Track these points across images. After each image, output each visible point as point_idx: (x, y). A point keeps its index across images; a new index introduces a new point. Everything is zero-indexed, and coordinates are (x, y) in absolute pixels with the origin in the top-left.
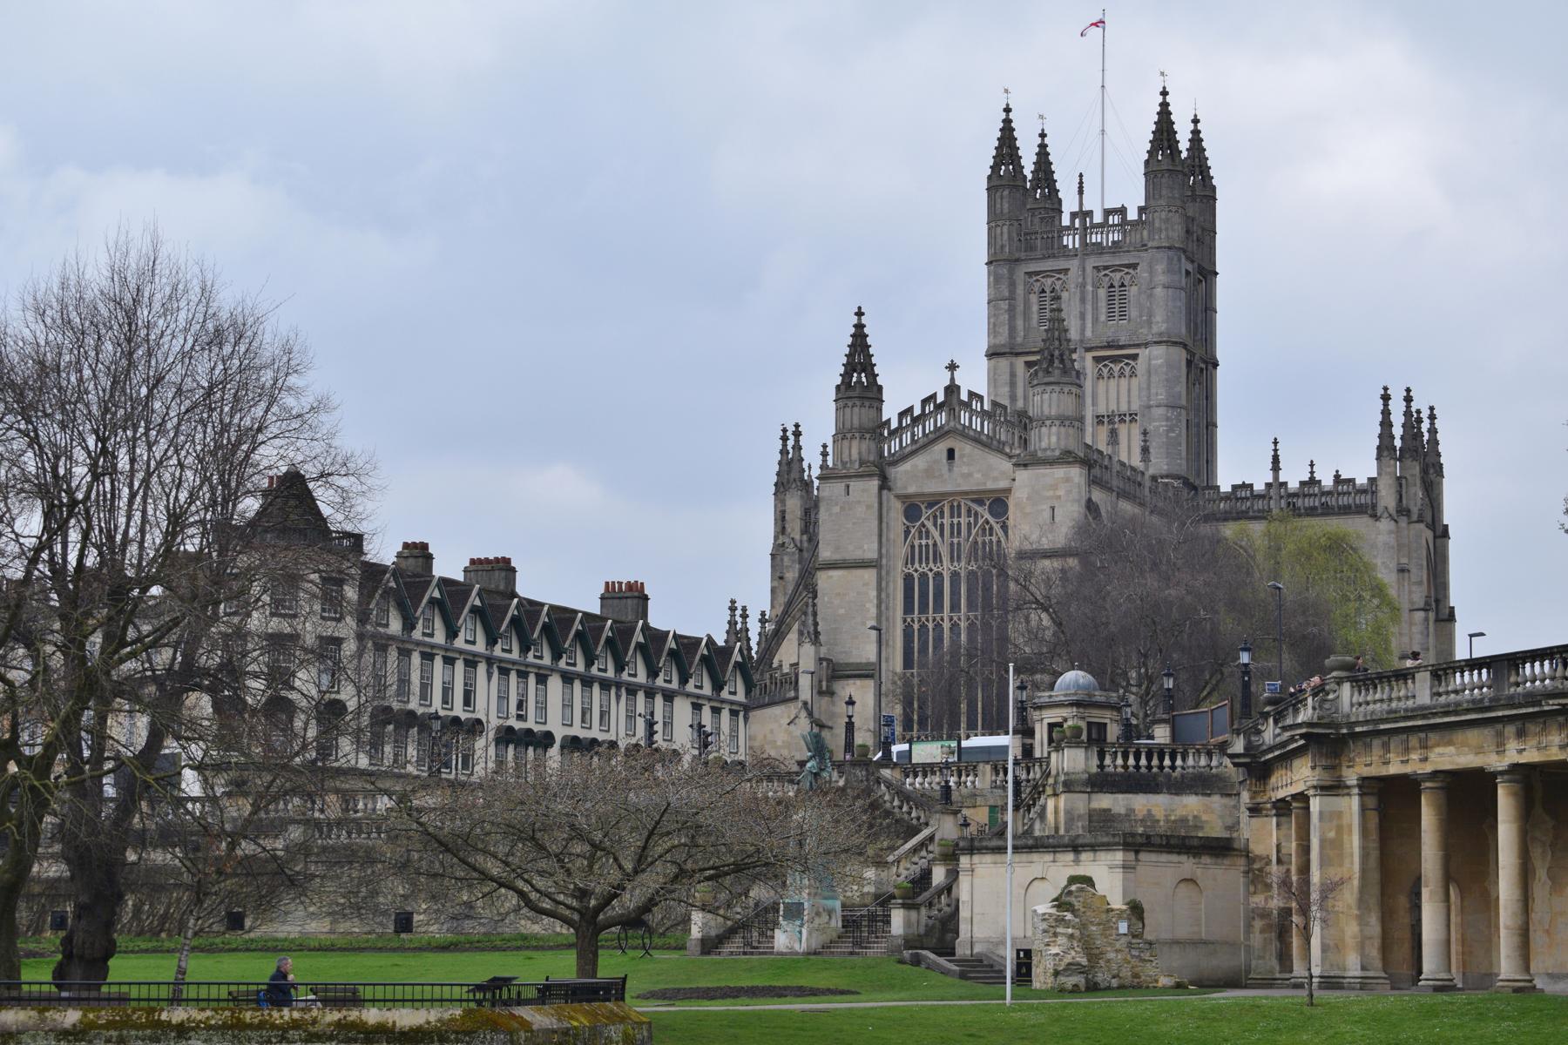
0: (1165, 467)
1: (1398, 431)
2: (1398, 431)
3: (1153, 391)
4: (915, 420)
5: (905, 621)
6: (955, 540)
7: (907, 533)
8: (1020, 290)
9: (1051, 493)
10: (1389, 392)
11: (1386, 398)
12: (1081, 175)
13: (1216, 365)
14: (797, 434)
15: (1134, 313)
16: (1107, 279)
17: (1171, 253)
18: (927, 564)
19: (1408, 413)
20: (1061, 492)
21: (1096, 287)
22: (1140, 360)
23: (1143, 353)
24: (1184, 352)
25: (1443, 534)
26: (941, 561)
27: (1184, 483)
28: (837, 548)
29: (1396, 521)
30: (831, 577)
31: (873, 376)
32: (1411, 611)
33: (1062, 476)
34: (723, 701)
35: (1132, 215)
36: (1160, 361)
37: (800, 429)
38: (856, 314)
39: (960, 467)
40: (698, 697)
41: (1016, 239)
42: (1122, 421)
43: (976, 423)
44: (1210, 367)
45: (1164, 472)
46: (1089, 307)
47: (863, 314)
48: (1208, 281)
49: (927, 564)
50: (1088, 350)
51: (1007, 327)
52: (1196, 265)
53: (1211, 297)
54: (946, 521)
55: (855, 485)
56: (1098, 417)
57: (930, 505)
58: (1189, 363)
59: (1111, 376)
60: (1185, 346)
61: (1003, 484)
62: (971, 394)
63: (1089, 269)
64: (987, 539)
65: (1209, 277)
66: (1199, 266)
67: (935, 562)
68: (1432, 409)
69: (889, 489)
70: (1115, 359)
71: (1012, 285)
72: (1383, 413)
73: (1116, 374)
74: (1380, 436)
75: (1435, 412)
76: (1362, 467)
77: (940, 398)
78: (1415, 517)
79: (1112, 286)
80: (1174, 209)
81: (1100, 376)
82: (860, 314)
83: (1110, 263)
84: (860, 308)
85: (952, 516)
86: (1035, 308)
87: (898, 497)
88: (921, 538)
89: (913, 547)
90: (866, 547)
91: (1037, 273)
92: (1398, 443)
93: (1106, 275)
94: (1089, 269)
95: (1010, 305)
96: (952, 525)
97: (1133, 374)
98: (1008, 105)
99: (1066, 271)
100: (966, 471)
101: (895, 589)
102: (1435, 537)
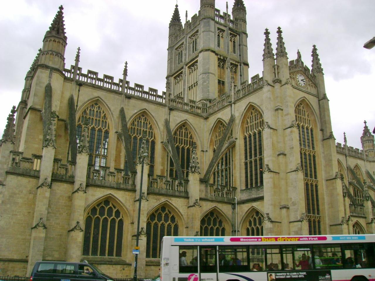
0: (202, 97)
1: (274, 46)
2: (274, 46)
10: (268, 31)
11: (267, 33)
12: (187, 11)
19: (280, 38)
24: (213, 54)
29: (274, 87)
46: (187, 51)
50: (186, 65)
58: (222, 61)
60: (213, 52)
70: (193, 65)
80: (207, 6)
92: (275, 52)
94: (188, 39)
95: (171, 61)
99: (183, 43)
102: (319, 101)
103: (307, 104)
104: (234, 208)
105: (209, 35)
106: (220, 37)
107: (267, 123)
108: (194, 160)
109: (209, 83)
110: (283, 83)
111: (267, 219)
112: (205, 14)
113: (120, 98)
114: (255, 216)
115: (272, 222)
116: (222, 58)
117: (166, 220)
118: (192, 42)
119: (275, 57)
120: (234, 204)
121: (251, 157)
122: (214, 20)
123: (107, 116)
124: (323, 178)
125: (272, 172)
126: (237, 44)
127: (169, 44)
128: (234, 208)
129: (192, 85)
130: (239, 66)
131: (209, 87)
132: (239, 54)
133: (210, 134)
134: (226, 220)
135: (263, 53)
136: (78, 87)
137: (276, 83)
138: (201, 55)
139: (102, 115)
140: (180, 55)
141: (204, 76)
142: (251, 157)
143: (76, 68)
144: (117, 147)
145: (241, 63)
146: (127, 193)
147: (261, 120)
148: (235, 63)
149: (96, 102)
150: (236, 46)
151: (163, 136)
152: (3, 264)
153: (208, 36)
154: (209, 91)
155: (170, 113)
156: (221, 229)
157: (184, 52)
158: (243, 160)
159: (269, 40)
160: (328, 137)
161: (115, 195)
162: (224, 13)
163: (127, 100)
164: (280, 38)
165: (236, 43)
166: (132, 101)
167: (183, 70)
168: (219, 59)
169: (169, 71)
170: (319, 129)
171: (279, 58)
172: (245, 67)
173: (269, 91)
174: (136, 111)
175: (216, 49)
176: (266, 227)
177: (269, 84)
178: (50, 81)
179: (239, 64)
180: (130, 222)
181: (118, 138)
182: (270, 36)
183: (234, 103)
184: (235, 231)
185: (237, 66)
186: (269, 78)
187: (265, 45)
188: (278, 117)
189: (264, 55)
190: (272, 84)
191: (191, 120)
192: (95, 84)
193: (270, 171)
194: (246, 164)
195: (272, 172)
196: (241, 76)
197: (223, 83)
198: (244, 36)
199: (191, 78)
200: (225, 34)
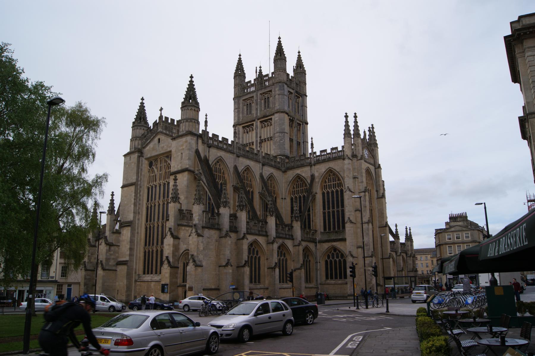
1: (352, 128)
2: (352, 128)
3: (276, 128)
8: (241, 105)
11: (346, 117)
13: (307, 124)
15: (271, 105)
16: (264, 97)
17: (280, 84)
19: (356, 122)
21: (261, 100)
22: (273, 119)
23: (273, 117)
24: (286, 116)
27: (286, 157)
29: (352, 160)
32: (359, 193)
33: (185, 140)
35: (270, 76)
36: (277, 119)
38: (141, 99)
39: (161, 145)
41: (240, 90)
42: (268, 140)
44: (304, 124)
45: (279, 154)
46: (259, 106)
47: (144, 99)
48: (303, 98)
50: (258, 119)
51: (237, 117)
52: (295, 91)
53: (304, 103)
58: (291, 121)
59: (265, 126)
60: (287, 113)
63: (259, 94)
65: (303, 96)
66: (296, 91)
68: (372, 125)
69: (143, 157)
70: (266, 121)
71: (239, 104)
72: (345, 122)
73: (266, 126)
74: (345, 130)
75: (373, 126)
76: (339, 142)
78: (359, 158)
79: (265, 99)
80: (281, 70)
81: (262, 127)
82: (143, 99)
84: (143, 97)
86: (245, 110)
87: (145, 159)
91: (245, 99)
92: (352, 132)
93: (264, 96)
94: (259, 94)
95: (238, 110)
97: (271, 125)
99: (253, 96)
100: (162, 146)
101: (143, 193)
102: (375, 169)
103: (369, 171)
104: (316, 246)
105: (284, 98)
106: (290, 99)
107: (348, 187)
108: (296, 212)
109: (284, 141)
110: (359, 158)
111: (349, 255)
112: (280, 78)
113: (233, 157)
114: (333, 252)
115: (353, 257)
116: (291, 118)
117: (281, 256)
118: (264, 99)
119: (352, 136)
120: (316, 243)
121: (329, 208)
122: (286, 84)
123: (225, 172)
124: (378, 226)
125: (353, 223)
126: (300, 105)
127: (235, 94)
128: (316, 246)
129: (266, 139)
130: (302, 125)
131: (285, 145)
132: (301, 114)
133: (289, 185)
134: (312, 254)
135: (343, 132)
136: (208, 148)
137: (354, 157)
138: (276, 115)
139: (222, 171)
140: (249, 106)
141: (280, 135)
142: (329, 208)
143: (205, 132)
144: (233, 198)
145: (303, 122)
146: (263, 238)
147: (339, 182)
148: (299, 122)
149: (220, 160)
150: (299, 107)
151: (259, 187)
152: (208, 292)
153: (283, 100)
154: (285, 148)
155: (262, 168)
156: (308, 260)
157: (253, 105)
158: (322, 210)
159: (348, 122)
160: (381, 196)
161: (258, 239)
162: (291, 76)
163: (237, 159)
164: (356, 122)
165: (299, 104)
166: (241, 159)
167: (254, 123)
168: (290, 119)
169: (237, 119)
170: (375, 190)
171: (356, 139)
172: (306, 125)
173: (349, 164)
174: (243, 168)
175: (288, 112)
176: (349, 261)
177: (349, 158)
178: (197, 146)
179: (302, 123)
180: (265, 259)
181: (234, 191)
182: (349, 119)
183: (314, 165)
184: (317, 262)
185: (300, 125)
186: (348, 153)
187: (345, 126)
188: (356, 184)
189: (344, 134)
190: (351, 158)
191: (277, 174)
192: (222, 147)
193: (351, 222)
194: (324, 213)
195: (353, 223)
196: (303, 133)
197: (292, 139)
198: (305, 97)
199: (264, 132)
200: (293, 96)
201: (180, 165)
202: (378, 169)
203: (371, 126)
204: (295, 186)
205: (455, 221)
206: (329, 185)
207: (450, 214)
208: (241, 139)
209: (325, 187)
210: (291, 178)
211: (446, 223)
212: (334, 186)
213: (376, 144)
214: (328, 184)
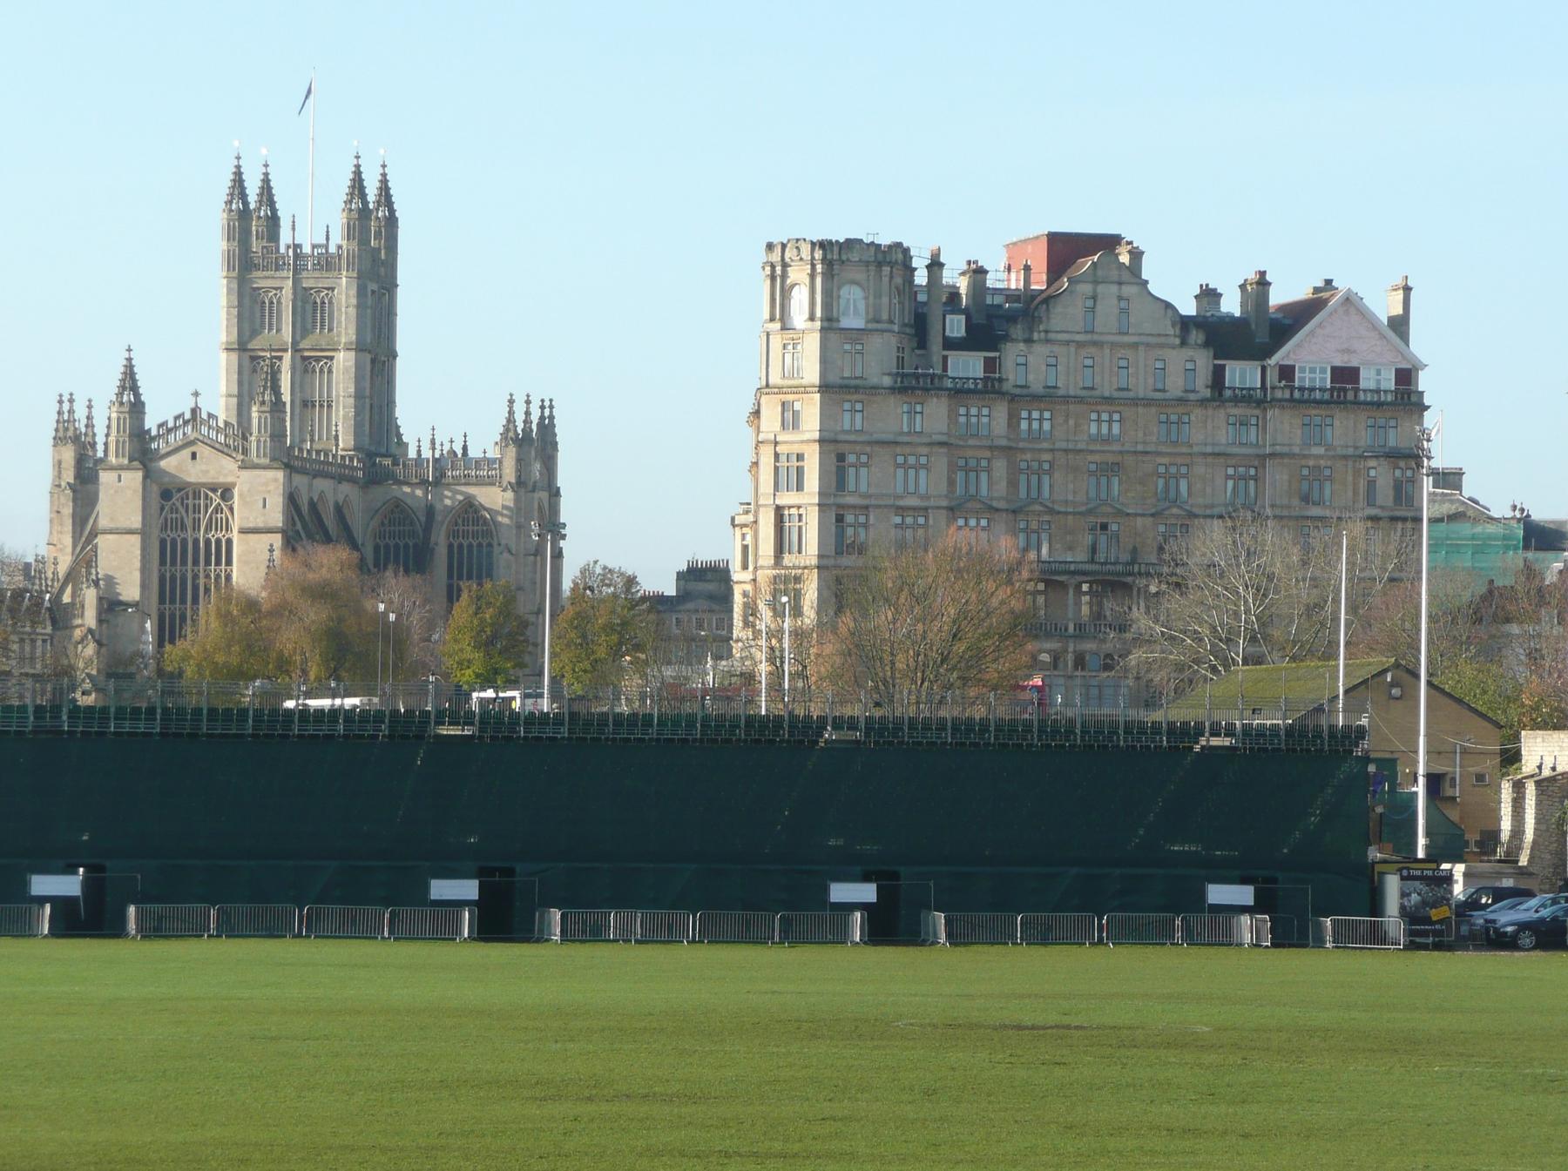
1: (520, 426)
4: (169, 431)
5: (160, 570)
6: (197, 516)
7: (162, 509)
9: (264, 488)
11: (511, 402)
13: (395, 356)
14: (71, 401)
18: (176, 531)
20: (271, 488)
25: (555, 493)
26: (186, 531)
28: (112, 519)
30: (108, 539)
31: (137, 395)
34: (38, 634)
37: (74, 397)
40: (23, 633)
43: (213, 434)
44: (390, 359)
46: (299, 318)
49: (176, 531)
54: (190, 502)
55: (124, 474)
56: (304, 401)
57: (179, 490)
58: (373, 361)
60: (370, 352)
61: (230, 479)
62: (210, 415)
64: (219, 516)
67: (182, 530)
75: (553, 403)
77: (188, 416)
78: (530, 488)
82: (129, 350)
83: (314, 286)
84: (129, 346)
85: (194, 499)
88: (172, 513)
89: (166, 519)
90: (133, 519)
96: (194, 505)
98: (239, 154)
168: (372, 359)
182: (515, 408)
201: (262, 519)
202: (555, 498)
203: (547, 404)
204: (386, 522)
205: (701, 580)
206: (463, 531)
207: (691, 559)
208: (246, 386)
209: (455, 534)
210: (379, 504)
211: (678, 573)
212: (475, 535)
213: (556, 443)
214: (461, 528)
